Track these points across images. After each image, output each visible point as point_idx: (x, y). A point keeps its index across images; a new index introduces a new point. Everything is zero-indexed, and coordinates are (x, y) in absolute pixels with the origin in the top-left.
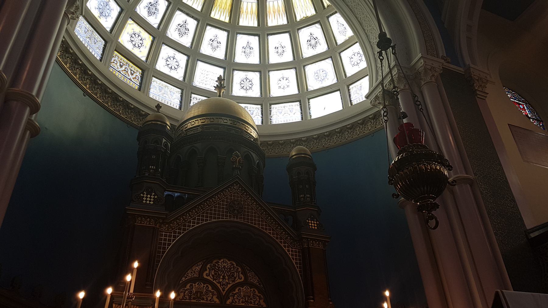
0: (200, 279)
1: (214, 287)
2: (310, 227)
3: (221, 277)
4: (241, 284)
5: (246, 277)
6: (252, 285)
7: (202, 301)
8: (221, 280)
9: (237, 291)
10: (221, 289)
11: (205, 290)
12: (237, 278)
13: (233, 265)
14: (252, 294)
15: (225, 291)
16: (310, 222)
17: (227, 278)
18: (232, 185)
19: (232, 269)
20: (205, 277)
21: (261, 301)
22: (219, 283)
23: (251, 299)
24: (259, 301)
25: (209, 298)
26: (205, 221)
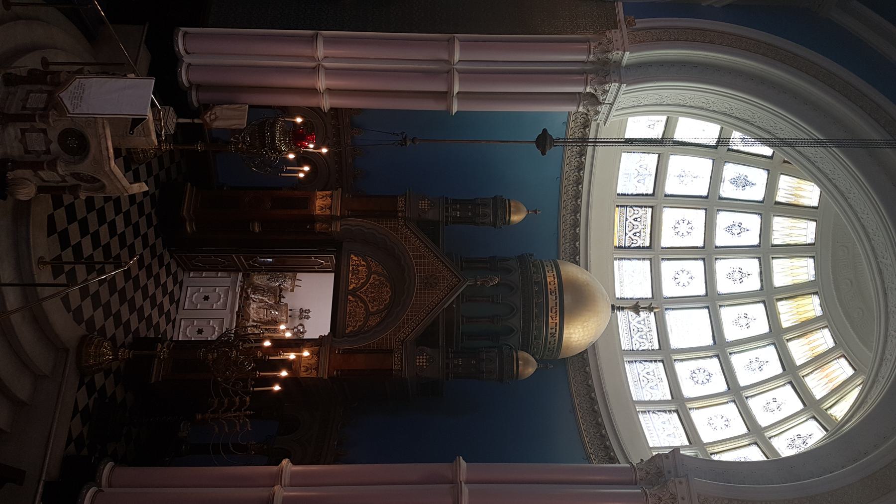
1: (363, 285)
2: (418, 357)
3: (373, 290)
4: (367, 309)
5: (374, 314)
7: (350, 275)
8: (370, 290)
9: (360, 304)
10: (361, 290)
11: (360, 277)
12: (373, 305)
13: (386, 301)
14: (358, 319)
15: (359, 294)
16: (425, 357)
17: (373, 295)
19: (381, 300)
20: (372, 276)
21: (351, 328)
23: (353, 318)
24: (351, 326)
25: (353, 281)
26: (408, 248)
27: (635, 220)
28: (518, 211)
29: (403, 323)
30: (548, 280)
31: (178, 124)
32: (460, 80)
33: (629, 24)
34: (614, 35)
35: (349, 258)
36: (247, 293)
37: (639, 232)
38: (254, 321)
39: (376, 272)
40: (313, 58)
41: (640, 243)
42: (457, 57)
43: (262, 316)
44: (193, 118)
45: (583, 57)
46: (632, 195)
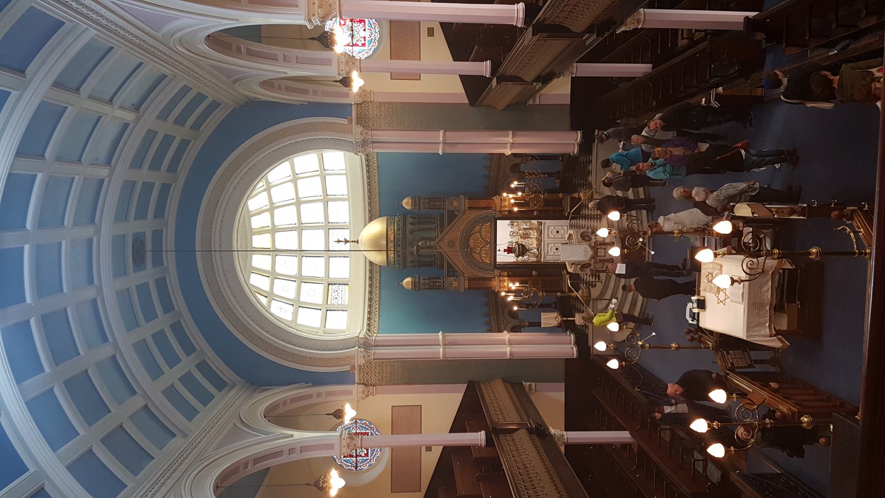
0: (480, 254)
1: (483, 247)
4: (481, 234)
5: (477, 232)
6: (481, 229)
9: (483, 237)
18: (439, 246)
21: (488, 224)
27: (337, 298)
28: (408, 282)
29: (464, 223)
31: (574, 317)
32: (438, 340)
33: (353, 367)
34: (362, 361)
36: (539, 252)
37: (334, 292)
39: (477, 254)
40: (512, 347)
41: (334, 287)
42: (441, 350)
43: (531, 240)
44: (567, 320)
45: (376, 351)
46: (339, 310)
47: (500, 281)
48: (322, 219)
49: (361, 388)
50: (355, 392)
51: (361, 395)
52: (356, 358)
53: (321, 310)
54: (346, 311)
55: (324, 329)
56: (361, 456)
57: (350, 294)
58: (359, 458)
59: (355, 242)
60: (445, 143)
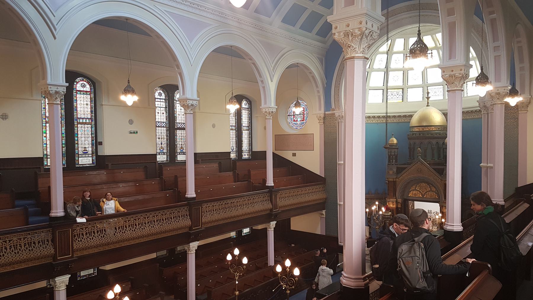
0: (415, 190)
1: (420, 192)
4: (429, 191)
20: (417, 189)
21: (436, 197)
22: (422, 191)
28: (393, 141)
30: (418, 130)
33: (334, 110)
35: (410, 197)
37: (397, 93)
38: (433, 228)
39: (415, 188)
41: (401, 92)
45: (343, 123)
46: (383, 97)
47: (393, 202)
48: (430, 82)
49: (322, 116)
50: (320, 112)
51: (319, 115)
52: (339, 111)
53: (384, 85)
54: (383, 102)
55: (368, 90)
56: (294, 117)
57: (393, 103)
58: (293, 116)
59: (428, 104)
60: (488, 168)
